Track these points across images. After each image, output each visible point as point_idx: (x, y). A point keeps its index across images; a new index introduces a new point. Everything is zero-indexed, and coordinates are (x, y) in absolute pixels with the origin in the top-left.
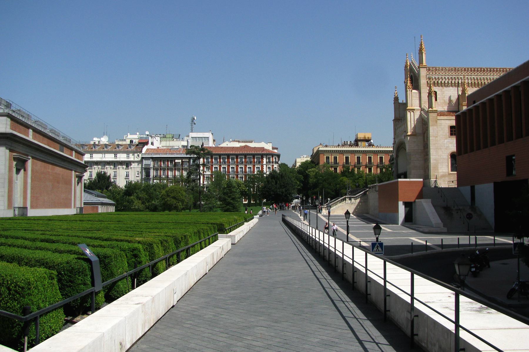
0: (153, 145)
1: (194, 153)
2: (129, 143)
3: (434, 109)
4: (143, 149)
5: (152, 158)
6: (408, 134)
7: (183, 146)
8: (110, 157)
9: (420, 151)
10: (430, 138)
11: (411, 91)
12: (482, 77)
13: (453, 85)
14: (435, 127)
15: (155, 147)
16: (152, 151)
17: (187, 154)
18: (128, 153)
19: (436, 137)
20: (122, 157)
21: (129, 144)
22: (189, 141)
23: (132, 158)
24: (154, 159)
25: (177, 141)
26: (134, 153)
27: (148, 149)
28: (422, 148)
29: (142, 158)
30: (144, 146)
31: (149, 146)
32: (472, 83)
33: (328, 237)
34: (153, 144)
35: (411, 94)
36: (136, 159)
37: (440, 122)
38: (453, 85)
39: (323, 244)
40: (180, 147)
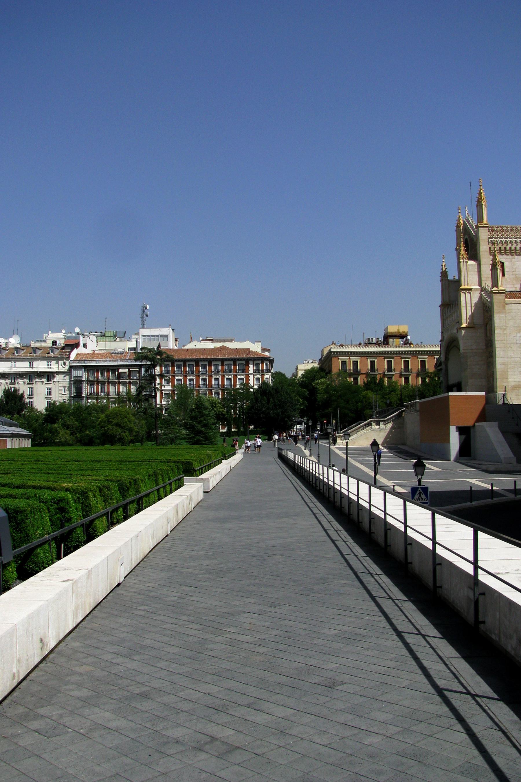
0: (86, 348)
1: (146, 358)
2: (50, 345)
3: (501, 288)
4: (71, 354)
5: (85, 367)
6: (462, 326)
7: (131, 349)
8: (22, 367)
9: (480, 351)
10: (496, 332)
11: (467, 262)
12: (504, 240)
13: (508, 252)
14: (503, 315)
15: (88, 351)
16: (85, 356)
17: (136, 360)
18: (49, 360)
19: (505, 330)
20: (41, 366)
21: (50, 347)
22: (138, 340)
23: (55, 367)
24: (87, 368)
25: (121, 341)
26: (57, 359)
27: (78, 354)
28: (484, 347)
29: (71, 367)
30: (72, 350)
31: (81, 350)
32: (502, 249)
33: (332, 473)
34: (86, 346)
35: (465, 268)
36: (62, 369)
37: (510, 308)
38: (508, 252)
39: (327, 482)
40: (127, 350)
